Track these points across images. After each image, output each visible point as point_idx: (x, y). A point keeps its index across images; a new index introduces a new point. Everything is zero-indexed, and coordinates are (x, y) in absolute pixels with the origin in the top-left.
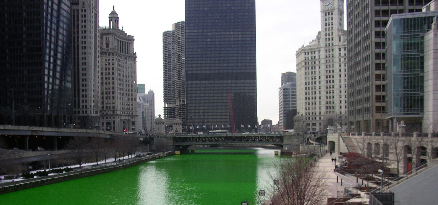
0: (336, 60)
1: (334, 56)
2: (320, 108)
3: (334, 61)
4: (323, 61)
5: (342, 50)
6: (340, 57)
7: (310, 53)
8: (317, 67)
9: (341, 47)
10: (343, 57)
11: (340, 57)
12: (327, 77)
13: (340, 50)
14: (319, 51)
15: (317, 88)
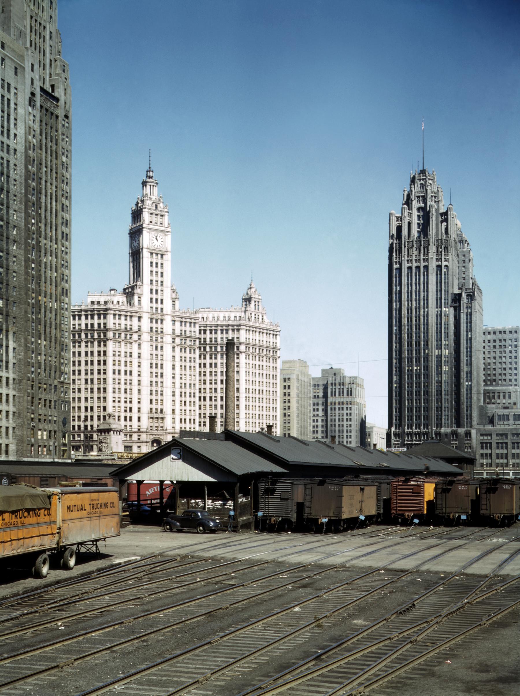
0: (168, 339)
1: (165, 331)
2: (139, 419)
3: (165, 340)
4: (146, 337)
5: (178, 324)
6: (174, 336)
7: (123, 318)
8: (135, 346)
9: (176, 319)
10: (178, 336)
11: (174, 336)
12: (151, 367)
13: (174, 325)
14: (139, 318)
15: (135, 382)
